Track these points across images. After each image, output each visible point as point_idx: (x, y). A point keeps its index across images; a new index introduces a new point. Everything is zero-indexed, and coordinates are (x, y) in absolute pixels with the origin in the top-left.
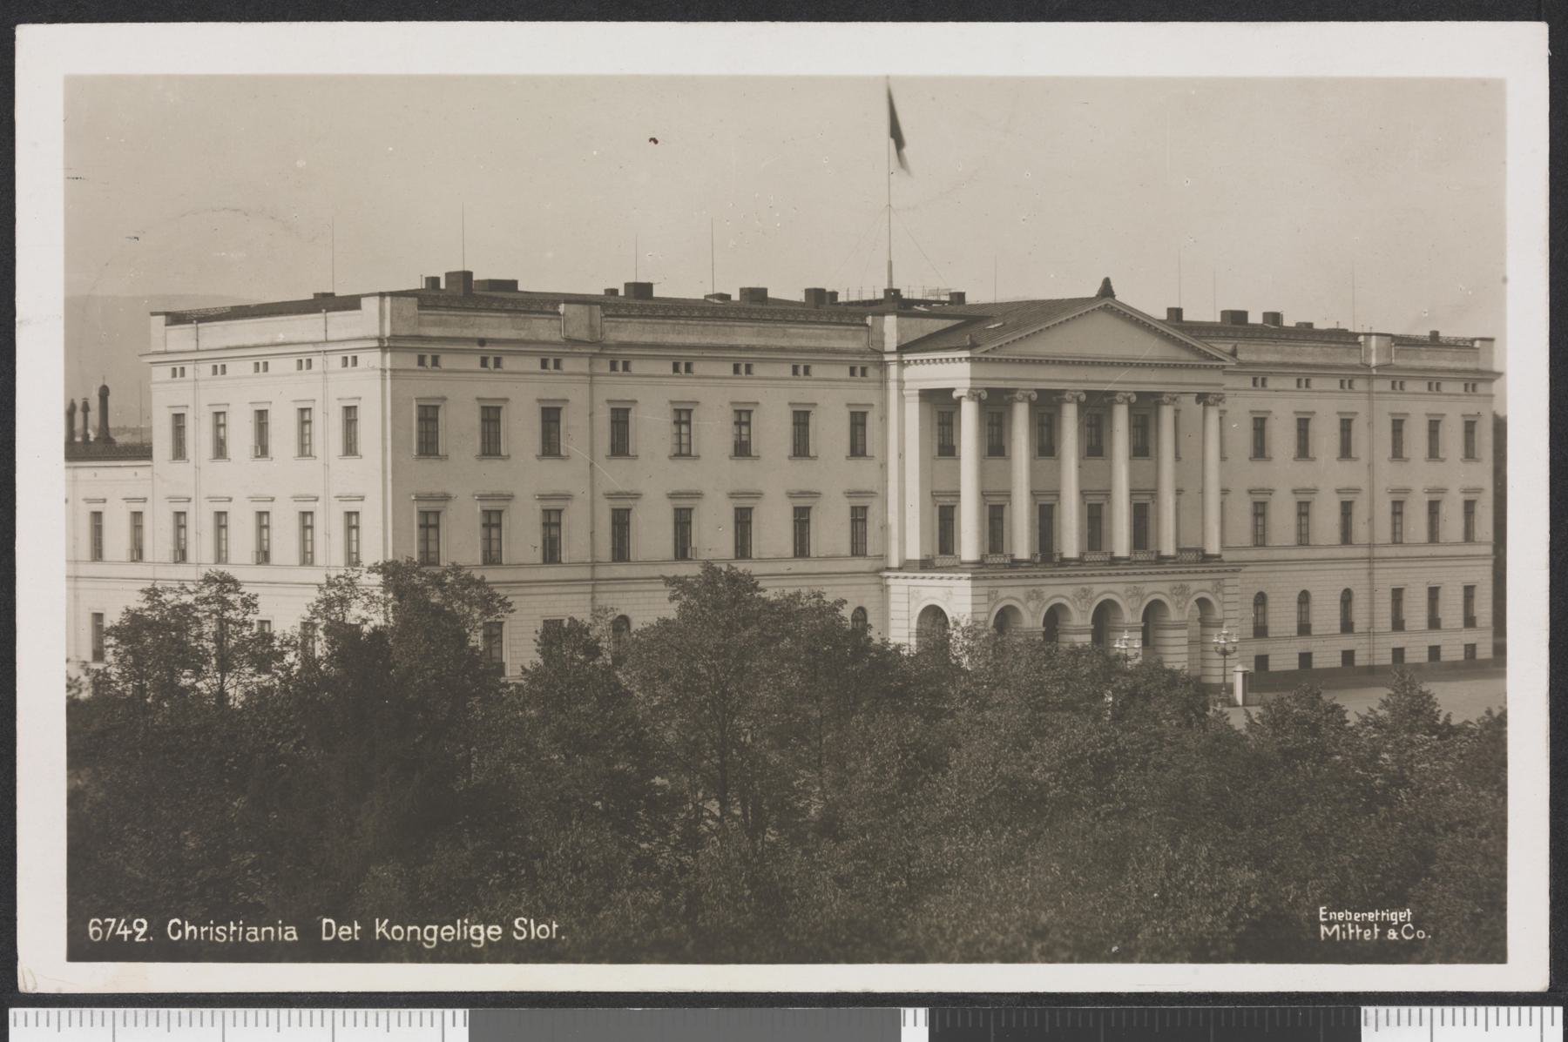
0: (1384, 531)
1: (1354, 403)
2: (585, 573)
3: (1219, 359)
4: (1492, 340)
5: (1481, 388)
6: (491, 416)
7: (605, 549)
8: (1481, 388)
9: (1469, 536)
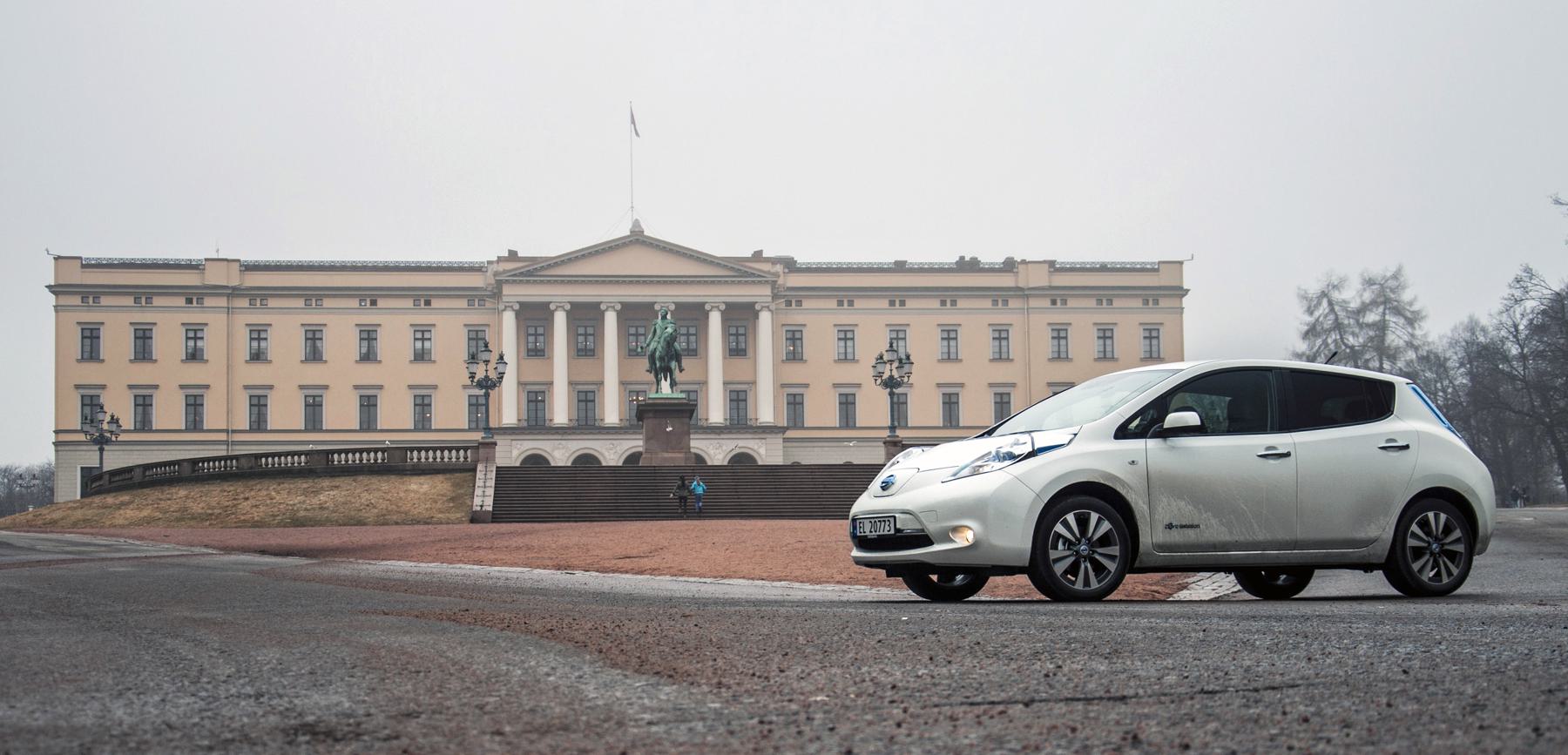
2: (223, 437)
4: (1181, 263)
6: (143, 336)
7: (242, 420)
8: (1163, 303)
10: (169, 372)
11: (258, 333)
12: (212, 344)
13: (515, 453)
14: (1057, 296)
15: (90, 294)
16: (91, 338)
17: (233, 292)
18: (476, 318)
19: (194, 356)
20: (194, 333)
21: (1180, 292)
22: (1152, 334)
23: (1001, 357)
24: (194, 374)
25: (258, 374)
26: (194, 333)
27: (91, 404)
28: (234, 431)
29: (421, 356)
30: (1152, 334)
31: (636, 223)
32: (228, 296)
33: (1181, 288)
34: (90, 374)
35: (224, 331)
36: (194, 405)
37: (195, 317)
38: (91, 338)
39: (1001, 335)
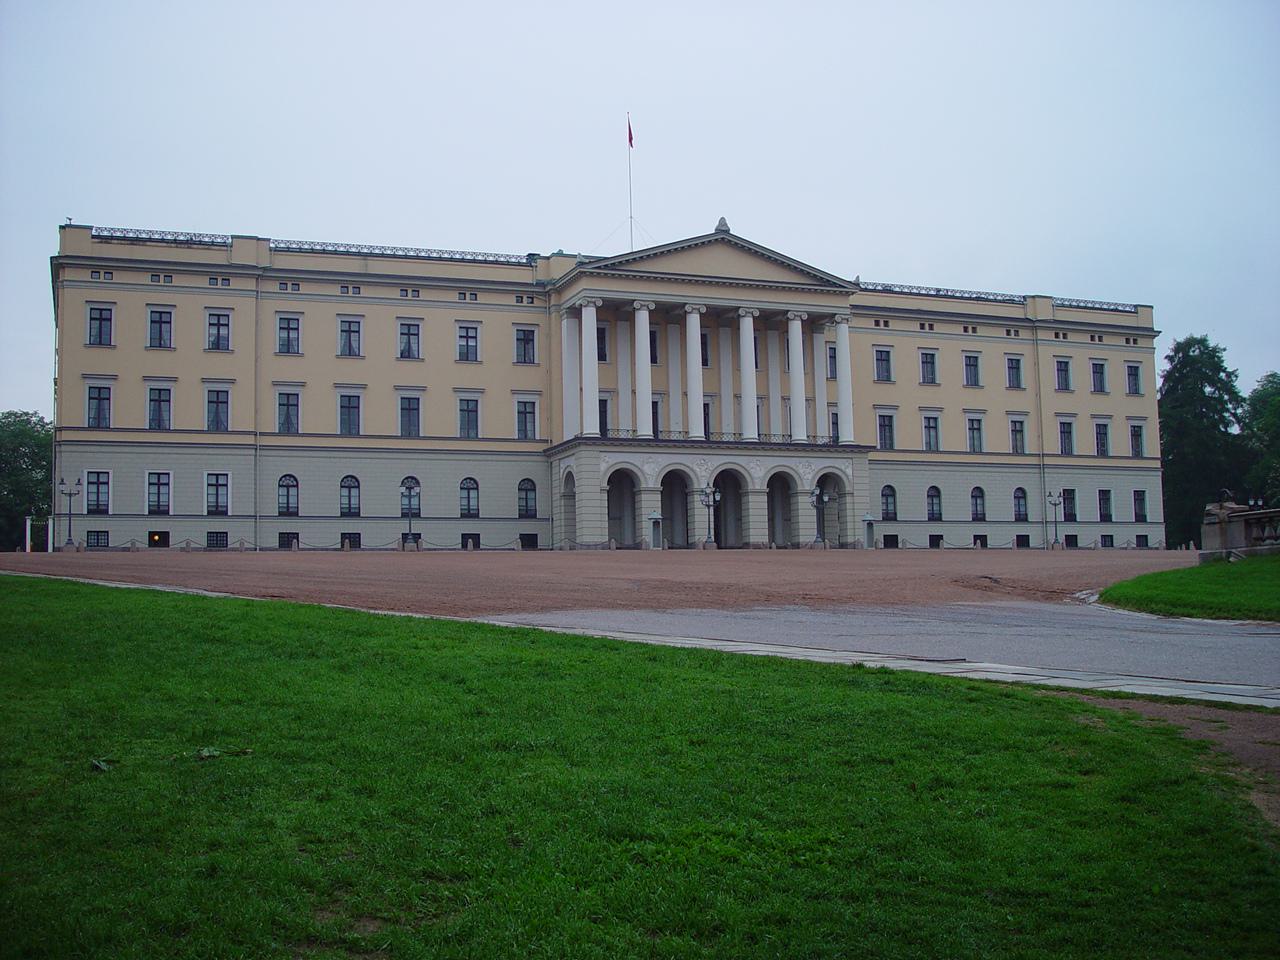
0: (1053, 444)
1: (1020, 347)
2: (250, 440)
3: (841, 286)
4: (1152, 307)
5: (1141, 342)
6: (161, 320)
7: (271, 420)
8: (1141, 342)
9: (1137, 452)
10: (189, 365)
11: (289, 324)
12: (240, 332)
13: (603, 467)
14: (1061, 330)
15: (102, 268)
16: (101, 318)
17: (262, 274)
18: (527, 316)
19: (219, 345)
20: (219, 320)
21: (1151, 333)
22: (1134, 372)
23: (1015, 384)
24: (218, 366)
25: (288, 369)
26: (219, 320)
27: (100, 397)
28: (262, 434)
29: (467, 355)
30: (1134, 372)
31: (723, 219)
32: (258, 278)
33: (1152, 329)
34: (100, 361)
35: (253, 318)
36: (218, 401)
37: (219, 301)
38: (101, 318)
39: (1014, 366)
